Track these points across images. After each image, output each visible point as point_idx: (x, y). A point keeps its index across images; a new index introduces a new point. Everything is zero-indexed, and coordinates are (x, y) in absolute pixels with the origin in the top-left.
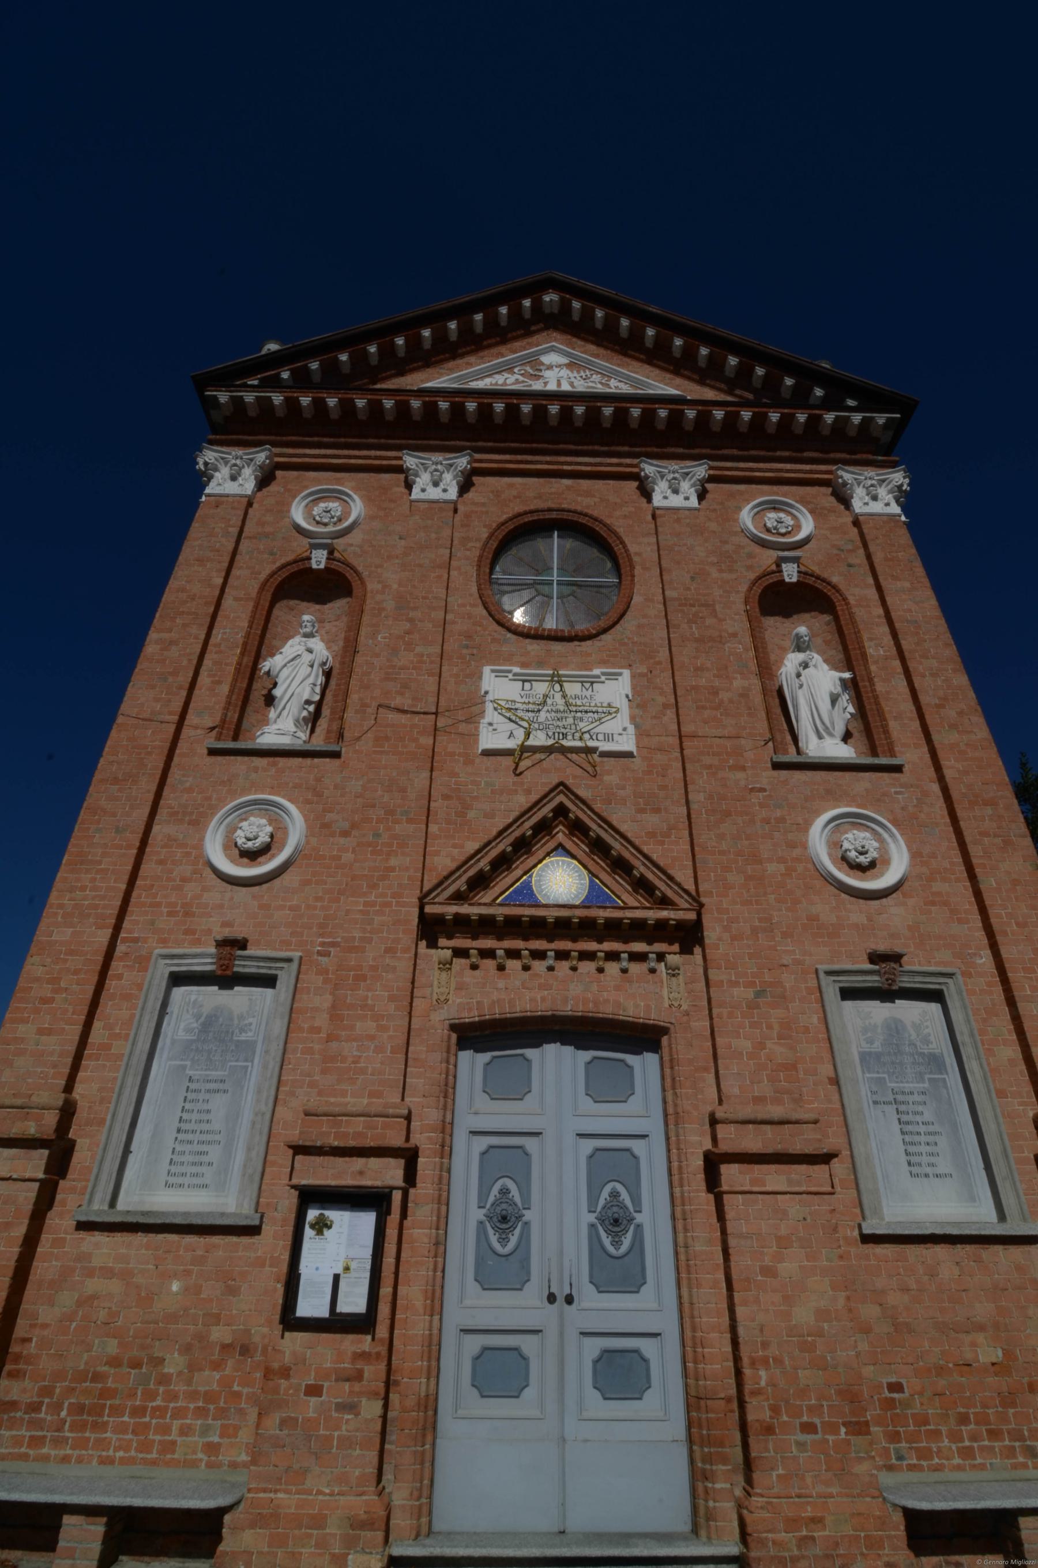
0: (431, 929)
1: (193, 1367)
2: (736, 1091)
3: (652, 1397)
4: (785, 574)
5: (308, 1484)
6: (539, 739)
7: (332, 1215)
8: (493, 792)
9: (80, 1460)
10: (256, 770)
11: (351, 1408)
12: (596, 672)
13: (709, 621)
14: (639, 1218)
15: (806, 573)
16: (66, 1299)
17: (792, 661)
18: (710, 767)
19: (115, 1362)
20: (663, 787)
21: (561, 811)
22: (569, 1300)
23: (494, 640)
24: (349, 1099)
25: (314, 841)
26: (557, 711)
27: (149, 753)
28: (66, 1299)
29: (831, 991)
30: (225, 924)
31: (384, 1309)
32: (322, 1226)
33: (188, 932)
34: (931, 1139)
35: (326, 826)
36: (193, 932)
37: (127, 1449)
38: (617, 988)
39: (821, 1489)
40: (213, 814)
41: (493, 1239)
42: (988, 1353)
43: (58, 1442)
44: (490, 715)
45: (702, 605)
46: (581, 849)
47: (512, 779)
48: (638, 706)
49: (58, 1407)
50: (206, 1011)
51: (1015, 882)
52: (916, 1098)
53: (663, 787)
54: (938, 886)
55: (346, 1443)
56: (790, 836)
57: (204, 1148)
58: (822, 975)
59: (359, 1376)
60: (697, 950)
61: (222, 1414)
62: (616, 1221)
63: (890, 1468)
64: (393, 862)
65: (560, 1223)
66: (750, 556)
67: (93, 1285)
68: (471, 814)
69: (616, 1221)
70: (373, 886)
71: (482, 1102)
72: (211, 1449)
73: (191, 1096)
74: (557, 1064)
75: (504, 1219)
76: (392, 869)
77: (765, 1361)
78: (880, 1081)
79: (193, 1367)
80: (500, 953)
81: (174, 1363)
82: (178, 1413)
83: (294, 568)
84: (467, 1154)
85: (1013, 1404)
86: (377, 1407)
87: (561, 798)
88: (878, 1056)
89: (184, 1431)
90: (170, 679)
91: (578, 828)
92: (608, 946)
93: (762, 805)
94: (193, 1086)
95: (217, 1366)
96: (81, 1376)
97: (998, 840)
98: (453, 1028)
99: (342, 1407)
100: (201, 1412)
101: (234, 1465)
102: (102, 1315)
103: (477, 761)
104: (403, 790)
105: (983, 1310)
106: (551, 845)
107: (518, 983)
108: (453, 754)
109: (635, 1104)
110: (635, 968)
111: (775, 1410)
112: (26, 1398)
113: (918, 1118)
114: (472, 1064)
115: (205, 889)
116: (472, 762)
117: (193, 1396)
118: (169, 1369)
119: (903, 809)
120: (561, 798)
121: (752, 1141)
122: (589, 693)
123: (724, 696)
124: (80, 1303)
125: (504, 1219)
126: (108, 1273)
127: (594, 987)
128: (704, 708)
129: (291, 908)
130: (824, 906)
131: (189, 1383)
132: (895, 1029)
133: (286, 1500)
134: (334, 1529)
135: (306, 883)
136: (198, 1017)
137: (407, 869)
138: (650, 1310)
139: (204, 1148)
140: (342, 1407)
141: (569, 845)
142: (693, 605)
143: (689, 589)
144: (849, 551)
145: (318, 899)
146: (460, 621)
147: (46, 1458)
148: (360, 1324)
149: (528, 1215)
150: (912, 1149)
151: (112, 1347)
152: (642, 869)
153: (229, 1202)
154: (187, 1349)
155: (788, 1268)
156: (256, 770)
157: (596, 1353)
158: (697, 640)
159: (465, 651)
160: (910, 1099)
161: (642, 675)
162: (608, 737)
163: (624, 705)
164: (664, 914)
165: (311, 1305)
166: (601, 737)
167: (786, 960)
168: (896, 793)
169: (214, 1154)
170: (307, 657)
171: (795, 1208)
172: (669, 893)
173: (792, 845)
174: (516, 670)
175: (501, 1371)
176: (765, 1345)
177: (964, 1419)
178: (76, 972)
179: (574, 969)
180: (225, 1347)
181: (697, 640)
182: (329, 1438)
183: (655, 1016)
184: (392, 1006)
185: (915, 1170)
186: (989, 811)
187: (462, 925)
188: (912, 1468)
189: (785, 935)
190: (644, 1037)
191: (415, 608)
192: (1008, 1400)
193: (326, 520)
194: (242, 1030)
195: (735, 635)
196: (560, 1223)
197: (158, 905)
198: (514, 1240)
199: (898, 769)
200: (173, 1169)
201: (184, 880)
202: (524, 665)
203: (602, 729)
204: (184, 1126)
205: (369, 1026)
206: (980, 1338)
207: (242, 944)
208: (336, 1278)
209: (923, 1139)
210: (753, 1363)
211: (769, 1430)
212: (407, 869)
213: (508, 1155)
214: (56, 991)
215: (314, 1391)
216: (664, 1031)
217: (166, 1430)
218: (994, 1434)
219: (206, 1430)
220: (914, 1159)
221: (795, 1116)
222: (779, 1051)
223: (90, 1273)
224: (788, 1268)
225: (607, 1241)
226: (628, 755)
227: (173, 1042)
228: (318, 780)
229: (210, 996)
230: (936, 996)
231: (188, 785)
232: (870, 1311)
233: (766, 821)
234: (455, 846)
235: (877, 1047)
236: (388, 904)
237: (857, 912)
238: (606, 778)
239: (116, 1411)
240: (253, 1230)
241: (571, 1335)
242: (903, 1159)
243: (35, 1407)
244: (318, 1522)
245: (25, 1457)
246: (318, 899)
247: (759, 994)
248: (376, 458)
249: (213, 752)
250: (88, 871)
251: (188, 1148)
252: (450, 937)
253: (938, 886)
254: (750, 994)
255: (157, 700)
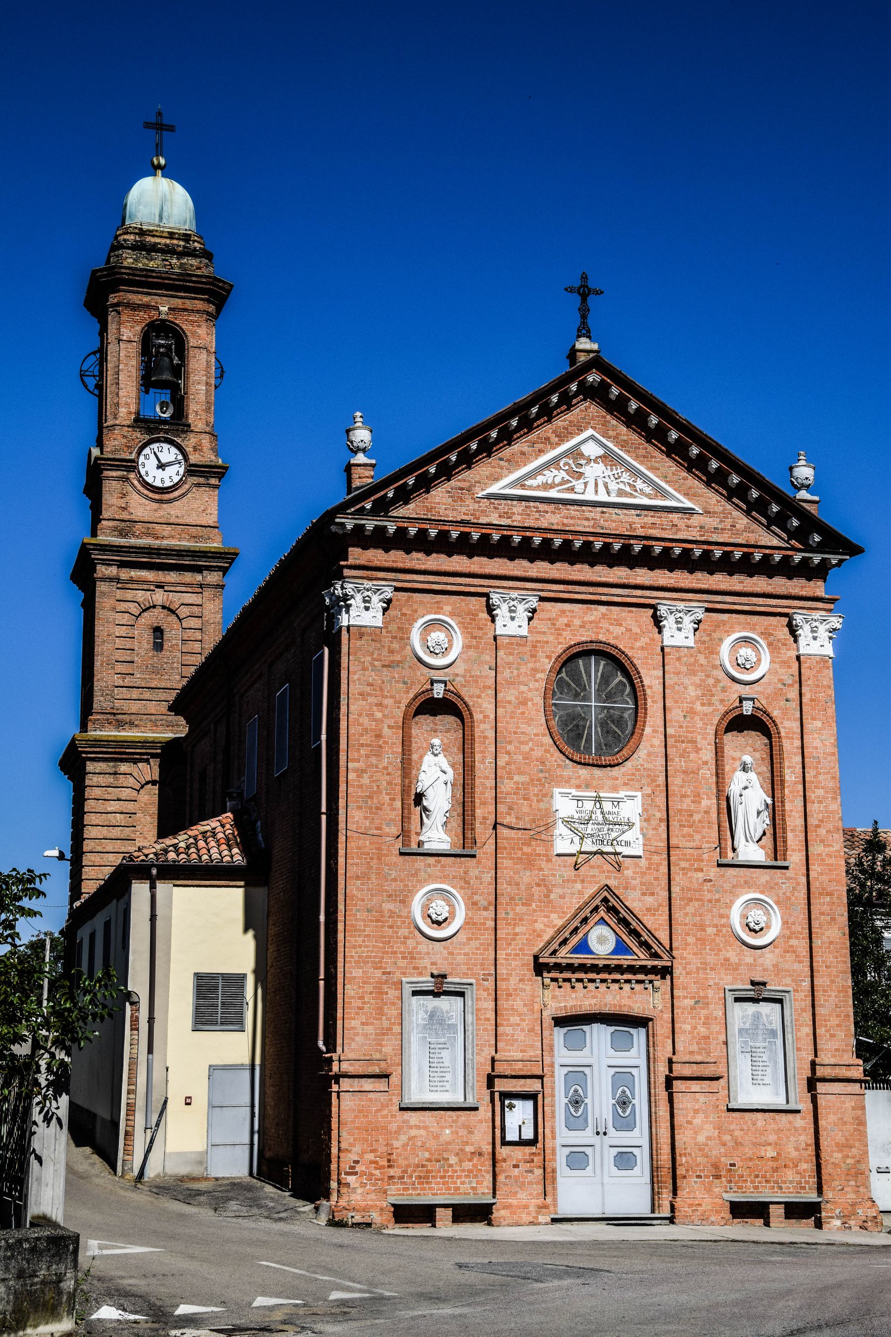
0: (540, 968)
1: (461, 1161)
2: (682, 1049)
3: (637, 1170)
4: (744, 708)
5: (519, 1196)
6: (589, 846)
7: (514, 1102)
8: (563, 881)
9: (424, 1195)
10: (429, 865)
11: (531, 1172)
12: (622, 794)
13: (692, 756)
14: (634, 1101)
15: (758, 708)
16: (403, 1138)
17: (739, 775)
18: (684, 869)
19: (429, 1160)
20: (656, 879)
21: (605, 900)
22: (605, 1134)
23: (559, 766)
24: (512, 1053)
25: (470, 913)
26: (598, 824)
27: (372, 859)
28: (403, 1138)
29: (730, 998)
30: (433, 964)
31: (540, 1138)
32: (511, 1107)
33: (414, 968)
34: (764, 1068)
35: (475, 904)
36: (417, 968)
37: (441, 1190)
38: (629, 997)
39: (701, 1196)
40: (413, 896)
41: (572, 1110)
42: (771, 1153)
43: (415, 1189)
44: (561, 829)
45: (689, 742)
46: (612, 921)
47: (574, 873)
48: (645, 820)
49: (411, 1177)
50: (429, 1009)
51: (831, 943)
52: (761, 1050)
53: (656, 879)
54: (794, 942)
55: (530, 1183)
56: (722, 911)
57: (443, 1074)
58: (727, 992)
59: (533, 1161)
60: (668, 977)
61: (475, 1176)
62: (624, 1103)
63: (726, 1192)
64: (517, 930)
65: (601, 1102)
66: (724, 690)
67: (413, 1132)
68: (552, 896)
69: (624, 1103)
70: (510, 944)
71: (564, 1052)
72: (473, 1188)
73: (432, 1051)
74: (600, 1033)
75: (576, 1102)
76: (517, 934)
77: (685, 1155)
78: (746, 1042)
79: (461, 1161)
80: (573, 980)
81: (453, 1160)
82: (458, 1177)
83: (422, 699)
84: (560, 1074)
85: (777, 1172)
86: (541, 1171)
87: (606, 894)
88: (747, 1030)
89: (463, 1183)
90: (369, 802)
91: (612, 910)
92: (627, 976)
93: (709, 891)
94: (432, 1046)
95: (470, 1160)
96: (417, 1166)
97: (828, 918)
98: (553, 1018)
99: (527, 1171)
100: (467, 1176)
101: (483, 1194)
102: (420, 1144)
103: (554, 860)
104: (518, 884)
105: (772, 1138)
106: (597, 918)
107: (582, 995)
108: (539, 855)
109: (634, 1051)
110: (638, 987)
111: (687, 1171)
112: (397, 1175)
113: (760, 1059)
114: (559, 1034)
115: (417, 943)
116: (551, 861)
117: (463, 1171)
118: (452, 1162)
119: (784, 894)
120: (606, 894)
121: (687, 1071)
122: (616, 810)
123: (697, 817)
124: (409, 1139)
125: (576, 1102)
126: (418, 1127)
127: (618, 997)
128: (684, 826)
129: (465, 954)
130: (733, 953)
131: (461, 1166)
132: (757, 1016)
133: (514, 1202)
134: (532, 1209)
135: (470, 939)
136: (426, 1012)
137: (525, 934)
138: (639, 1136)
139: (443, 1074)
140: (527, 1171)
141: (606, 918)
142: (683, 742)
143: (681, 727)
144: (789, 685)
145: (478, 949)
146: (536, 748)
147: (411, 1194)
148: (533, 1142)
149: (586, 1101)
150: (755, 1073)
151: (427, 1155)
152: (646, 937)
153: (455, 1097)
154: (457, 1154)
155: (697, 1121)
156: (429, 865)
157: (615, 1154)
158: (685, 772)
159: (541, 775)
160: (758, 1050)
161: (649, 796)
162: (627, 844)
163: (636, 819)
164: (656, 963)
165: (512, 1136)
166: (623, 844)
167: (711, 983)
168: (782, 883)
169: (448, 1076)
170: (444, 777)
171: (702, 1098)
172: (659, 951)
173: (721, 916)
174: (574, 792)
175: (578, 1159)
176: (685, 1149)
177: (757, 1176)
178: (371, 993)
179: (608, 988)
180: (472, 1153)
181: (685, 772)
182: (524, 1182)
183: (647, 1013)
184: (526, 1009)
185: (754, 1082)
186: (828, 899)
187: (558, 967)
188: (734, 1192)
189: (712, 969)
190: (641, 1022)
191: (510, 743)
192: (775, 1170)
193: (437, 651)
194: (449, 1019)
195: (706, 763)
196: (601, 1102)
197: (396, 953)
198: (581, 1111)
199: (786, 868)
200: (432, 1084)
201: (405, 938)
202: (578, 787)
203: (624, 837)
204: (432, 1065)
205: (514, 1019)
206: (769, 1148)
207: (444, 976)
208: (520, 1126)
209: (760, 1068)
210: (680, 1155)
211: (685, 1177)
212: (525, 934)
213: (578, 1075)
214: (364, 1003)
215: (516, 1166)
216: (651, 1020)
217: (455, 1183)
218: (767, 1181)
219: (470, 1182)
220: (755, 1077)
221: (707, 1060)
222: (702, 1030)
223: (411, 1127)
224: (697, 1121)
225: (620, 1111)
226: (640, 857)
227: (417, 1025)
228: (466, 873)
229: (430, 1002)
230: (780, 1001)
231: (393, 876)
232: (727, 1138)
233: (710, 901)
234: (545, 916)
235: (747, 1026)
236: (517, 955)
237: (749, 956)
238: (626, 872)
239: (434, 1177)
240: (476, 1109)
241: (606, 1147)
242: (751, 1077)
243: (403, 1177)
244: (526, 1207)
245: (403, 1195)
246: (478, 949)
247: (696, 1003)
248: (466, 585)
249: (401, 854)
250: (359, 936)
251: (436, 1074)
252: (549, 972)
253: (794, 942)
254: (692, 1002)
255: (366, 818)
